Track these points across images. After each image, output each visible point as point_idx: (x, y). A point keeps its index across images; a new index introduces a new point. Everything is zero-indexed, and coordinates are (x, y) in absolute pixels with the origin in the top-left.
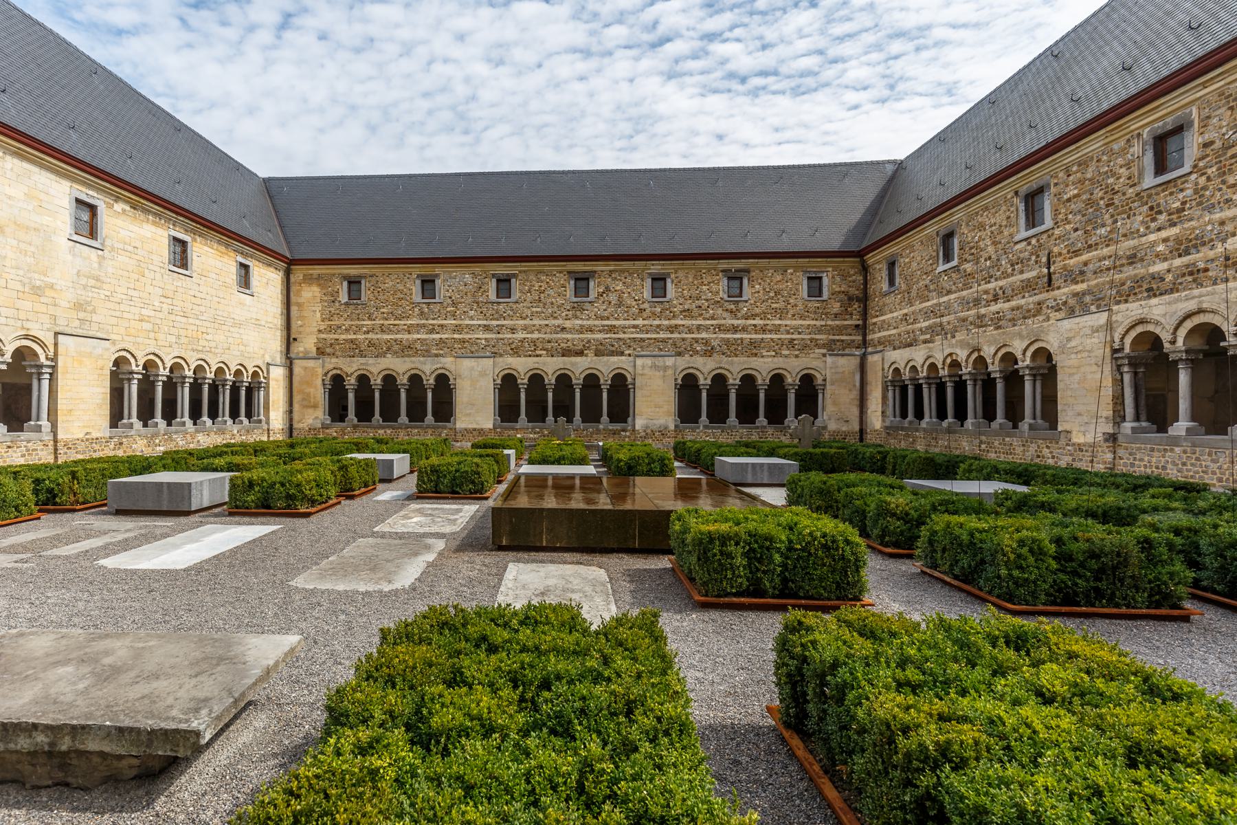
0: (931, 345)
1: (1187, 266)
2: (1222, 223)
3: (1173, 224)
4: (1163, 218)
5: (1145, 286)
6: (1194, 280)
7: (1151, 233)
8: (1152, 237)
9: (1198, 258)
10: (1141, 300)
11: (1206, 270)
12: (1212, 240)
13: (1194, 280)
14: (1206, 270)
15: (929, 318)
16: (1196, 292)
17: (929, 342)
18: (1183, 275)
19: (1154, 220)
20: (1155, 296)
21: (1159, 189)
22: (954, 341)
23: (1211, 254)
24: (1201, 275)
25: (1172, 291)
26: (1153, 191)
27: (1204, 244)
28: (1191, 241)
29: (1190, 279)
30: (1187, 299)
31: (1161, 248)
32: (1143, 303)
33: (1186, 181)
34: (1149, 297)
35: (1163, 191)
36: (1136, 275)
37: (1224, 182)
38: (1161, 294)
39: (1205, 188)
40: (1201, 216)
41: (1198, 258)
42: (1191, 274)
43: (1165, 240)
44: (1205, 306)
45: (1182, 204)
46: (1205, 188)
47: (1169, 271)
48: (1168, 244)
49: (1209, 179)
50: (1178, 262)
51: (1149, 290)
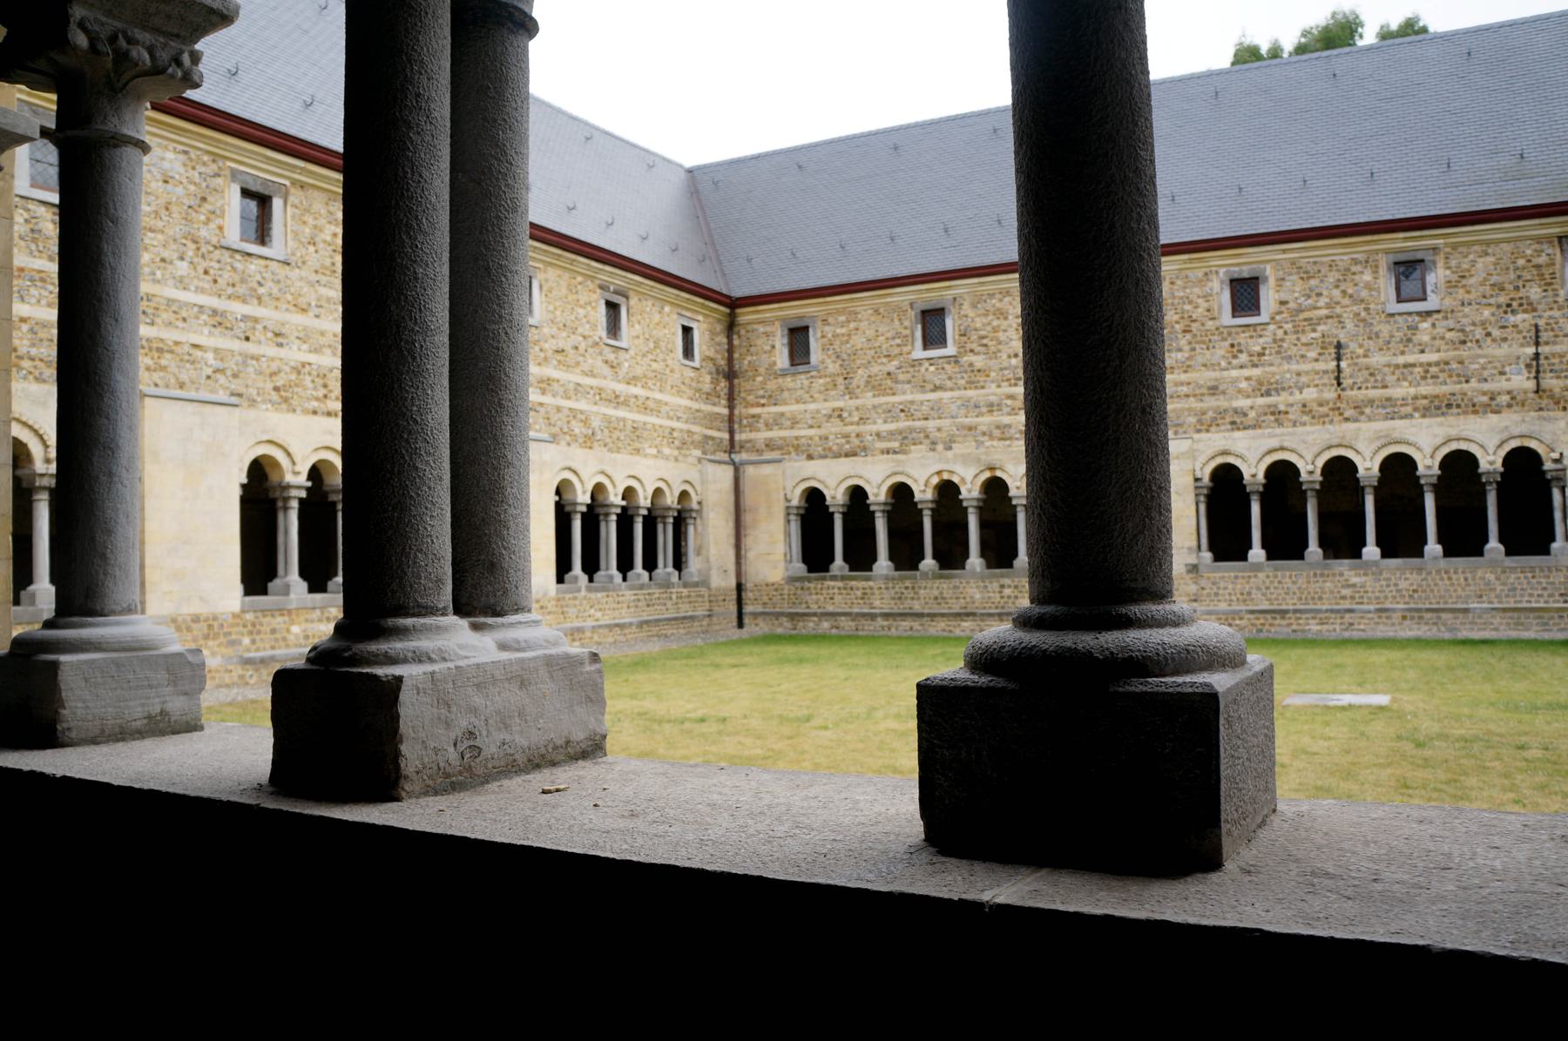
0: (899, 457)
1: (1269, 406)
2: (1299, 374)
3: (1254, 366)
4: (1243, 358)
5: (1228, 419)
6: (1276, 420)
7: (1233, 368)
8: (1234, 373)
9: (1280, 400)
10: (1224, 431)
11: (1287, 413)
12: (1290, 387)
13: (1276, 420)
14: (1287, 413)
15: (896, 419)
16: (1278, 431)
17: (895, 452)
18: (1266, 414)
19: (1235, 357)
20: (1238, 429)
21: (1240, 329)
22: (950, 454)
23: (1291, 399)
24: (1282, 416)
25: (1254, 427)
26: (1234, 330)
27: (1283, 389)
28: (1272, 384)
29: (1272, 418)
30: (1271, 436)
31: (1244, 385)
32: (1226, 434)
33: (1265, 330)
34: (1233, 430)
35: (1244, 332)
36: (1219, 407)
37: (1298, 339)
38: (1245, 428)
39: (1282, 340)
40: (1280, 364)
41: (1280, 400)
42: (1273, 413)
43: (1248, 379)
44: (1286, 444)
45: (1264, 349)
46: (1282, 340)
47: (1252, 408)
48: (1251, 382)
49: (1286, 333)
50: (1261, 401)
51: (1233, 423)
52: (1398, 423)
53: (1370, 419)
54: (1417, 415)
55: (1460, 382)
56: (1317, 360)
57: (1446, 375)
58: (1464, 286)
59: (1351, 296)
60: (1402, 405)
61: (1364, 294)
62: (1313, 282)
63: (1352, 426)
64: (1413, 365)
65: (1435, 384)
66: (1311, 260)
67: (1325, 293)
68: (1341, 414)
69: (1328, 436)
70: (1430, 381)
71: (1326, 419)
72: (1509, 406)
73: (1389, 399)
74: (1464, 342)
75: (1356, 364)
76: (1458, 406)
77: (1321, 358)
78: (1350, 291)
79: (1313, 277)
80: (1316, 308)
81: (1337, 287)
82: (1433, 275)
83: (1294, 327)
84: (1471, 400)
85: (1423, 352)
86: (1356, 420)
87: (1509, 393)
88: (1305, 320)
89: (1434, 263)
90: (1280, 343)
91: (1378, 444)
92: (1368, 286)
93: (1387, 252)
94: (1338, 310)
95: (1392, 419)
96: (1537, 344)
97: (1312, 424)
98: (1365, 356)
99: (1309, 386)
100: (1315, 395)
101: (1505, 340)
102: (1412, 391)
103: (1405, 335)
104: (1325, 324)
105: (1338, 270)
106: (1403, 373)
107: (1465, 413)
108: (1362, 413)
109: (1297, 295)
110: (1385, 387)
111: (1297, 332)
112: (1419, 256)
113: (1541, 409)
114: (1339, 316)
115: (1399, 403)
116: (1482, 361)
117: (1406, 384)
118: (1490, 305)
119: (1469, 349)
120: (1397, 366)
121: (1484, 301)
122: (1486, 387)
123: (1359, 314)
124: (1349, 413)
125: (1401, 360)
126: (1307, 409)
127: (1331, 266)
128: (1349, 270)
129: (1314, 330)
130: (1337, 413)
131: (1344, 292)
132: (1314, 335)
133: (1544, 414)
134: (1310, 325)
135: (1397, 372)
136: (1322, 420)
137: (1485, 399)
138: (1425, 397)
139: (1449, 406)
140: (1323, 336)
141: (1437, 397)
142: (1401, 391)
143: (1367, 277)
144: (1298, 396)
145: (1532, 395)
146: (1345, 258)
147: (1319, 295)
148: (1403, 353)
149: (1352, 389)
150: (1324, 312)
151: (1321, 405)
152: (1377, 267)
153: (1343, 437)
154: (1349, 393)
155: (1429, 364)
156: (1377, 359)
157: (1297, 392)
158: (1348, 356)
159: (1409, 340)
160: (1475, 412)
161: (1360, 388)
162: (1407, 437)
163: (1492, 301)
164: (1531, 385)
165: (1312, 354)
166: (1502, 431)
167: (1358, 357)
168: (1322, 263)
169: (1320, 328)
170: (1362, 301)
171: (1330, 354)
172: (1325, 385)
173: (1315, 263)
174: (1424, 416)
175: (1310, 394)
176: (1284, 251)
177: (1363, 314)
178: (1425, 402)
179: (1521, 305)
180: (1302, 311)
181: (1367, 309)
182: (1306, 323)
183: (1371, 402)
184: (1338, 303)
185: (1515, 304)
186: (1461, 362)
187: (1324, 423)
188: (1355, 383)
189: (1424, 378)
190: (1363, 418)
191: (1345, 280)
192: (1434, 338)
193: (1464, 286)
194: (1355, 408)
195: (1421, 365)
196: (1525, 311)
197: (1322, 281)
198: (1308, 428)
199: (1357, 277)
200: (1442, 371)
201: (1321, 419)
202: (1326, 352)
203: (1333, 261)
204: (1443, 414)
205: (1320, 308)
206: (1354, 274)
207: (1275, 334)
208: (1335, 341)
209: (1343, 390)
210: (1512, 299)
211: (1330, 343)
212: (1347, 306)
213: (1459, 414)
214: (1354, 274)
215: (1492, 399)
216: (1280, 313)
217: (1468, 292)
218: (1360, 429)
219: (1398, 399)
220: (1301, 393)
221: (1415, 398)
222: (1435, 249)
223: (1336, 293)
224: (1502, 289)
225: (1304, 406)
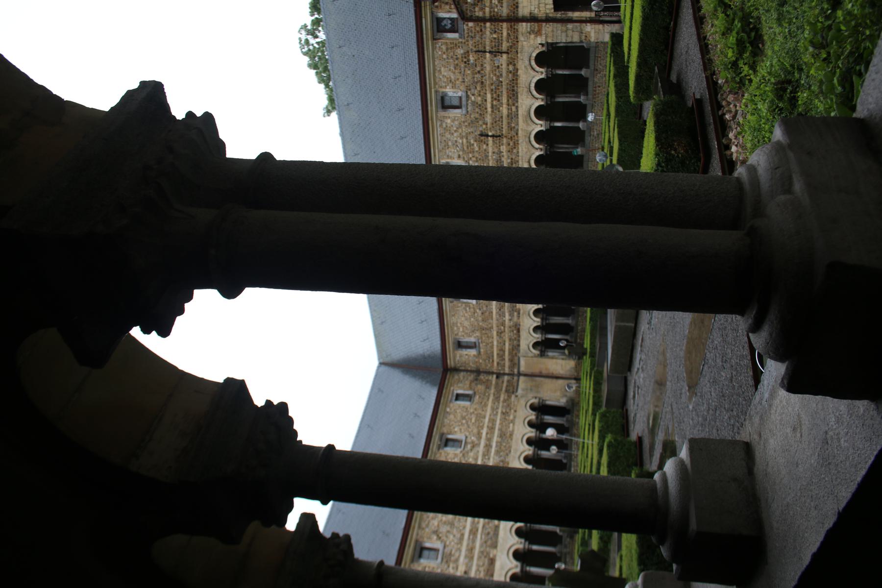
11: (512, 159)
12: (500, 157)
14: (512, 159)
27: (500, 160)
37: (477, 151)
39: (477, 158)
46: (477, 158)
49: (473, 157)
52: (520, 112)
53: (518, 124)
54: (516, 104)
55: (502, 85)
56: (487, 145)
57: (497, 91)
58: (455, 81)
59: (457, 128)
60: (511, 110)
61: (456, 123)
62: (450, 144)
63: (520, 132)
64: (492, 105)
65: (502, 96)
66: (439, 143)
67: (455, 139)
68: (514, 136)
69: (524, 143)
70: (500, 98)
71: (516, 143)
72: (514, 65)
73: (508, 116)
74: (482, 83)
75: (490, 128)
76: (513, 87)
77: (486, 142)
78: (455, 129)
79: (448, 143)
80: (462, 143)
81: (453, 134)
82: (449, 93)
83: (471, 153)
84: (510, 81)
85: (486, 100)
86: (518, 130)
87: (508, 65)
88: (468, 148)
89: (443, 92)
90: (478, 159)
91: (529, 122)
92: (453, 121)
93: (437, 111)
94: (464, 134)
95: (518, 115)
96: (485, 52)
97: (518, 149)
98: (487, 124)
99: (500, 149)
100: (504, 147)
101: (482, 65)
102: (505, 106)
103: (477, 107)
104: (470, 140)
105: (445, 133)
106: (496, 109)
107: (517, 84)
108: (514, 127)
109: (455, 151)
110: (502, 117)
111: (473, 152)
112: (439, 98)
113: (517, 52)
114: (467, 134)
115: (510, 111)
116: (492, 75)
117: (501, 108)
118: (464, 71)
119: (486, 80)
120: (492, 111)
121: (462, 73)
122: (504, 74)
123: (466, 126)
124: (513, 133)
125: (489, 110)
126: (511, 150)
127: (442, 136)
128: (445, 128)
129: (473, 145)
130: (513, 138)
131: (456, 131)
132: (475, 145)
133: (519, 50)
134: (470, 146)
135: (495, 111)
136: (516, 145)
137: (510, 75)
138: (508, 100)
139: (513, 90)
140: (476, 141)
141: (508, 96)
142: (505, 111)
143: (449, 121)
144: (505, 154)
145: (510, 56)
146: (439, 129)
147: (456, 141)
148: (486, 109)
149: (502, 131)
150: (465, 140)
151: (509, 144)
152: (444, 117)
153: (525, 136)
154: (504, 132)
155: (492, 98)
156: (489, 119)
157: (502, 154)
158: (486, 131)
159: (480, 105)
160: (517, 80)
161: (502, 128)
162: (527, 109)
163: (463, 70)
164: (505, 56)
165: (485, 147)
166: (527, 69)
167: (487, 127)
168: (441, 139)
169: (472, 142)
170: (460, 124)
171: (485, 139)
172: (499, 142)
173: (441, 142)
174: (517, 102)
175: (504, 148)
176: (435, 156)
177: (466, 124)
178: (510, 100)
179: (465, 58)
180: (463, 148)
181: (464, 122)
182: (469, 148)
183: (508, 123)
184: (460, 134)
185: (465, 60)
186: (492, 84)
187: (518, 144)
188: (499, 129)
189: (499, 100)
190: (516, 127)
191: (450, 130)
192: (480, 95)
193: (455, 81)
194: (511, 130)
195: (492, 101)
196: (469, 56)
197: (450, 140)
198: (520, 150)
199: (449, 125)
200: (496, 92)
201: (516, 144)
202: (483, 140)
203: (440, 135)
204: (517, 93)
205: (462, 142)
206: (447, 126)
207: (474, 161)
208: (478, 136)
209: (502, 135)
210: (462, 61)
211: (479, 138)
212: (462, 130)
213: (517, 87)
214: (447, 126)
215: (511, 72)
216: (464, 158)
217: (458, 79)
218: (522, 129)
219: (508, 112)
220: (503, 152)
221: (508, 105)
222: (436, 92)
223: (455, 135)
224: (457, 65)
225: (509, 151)
